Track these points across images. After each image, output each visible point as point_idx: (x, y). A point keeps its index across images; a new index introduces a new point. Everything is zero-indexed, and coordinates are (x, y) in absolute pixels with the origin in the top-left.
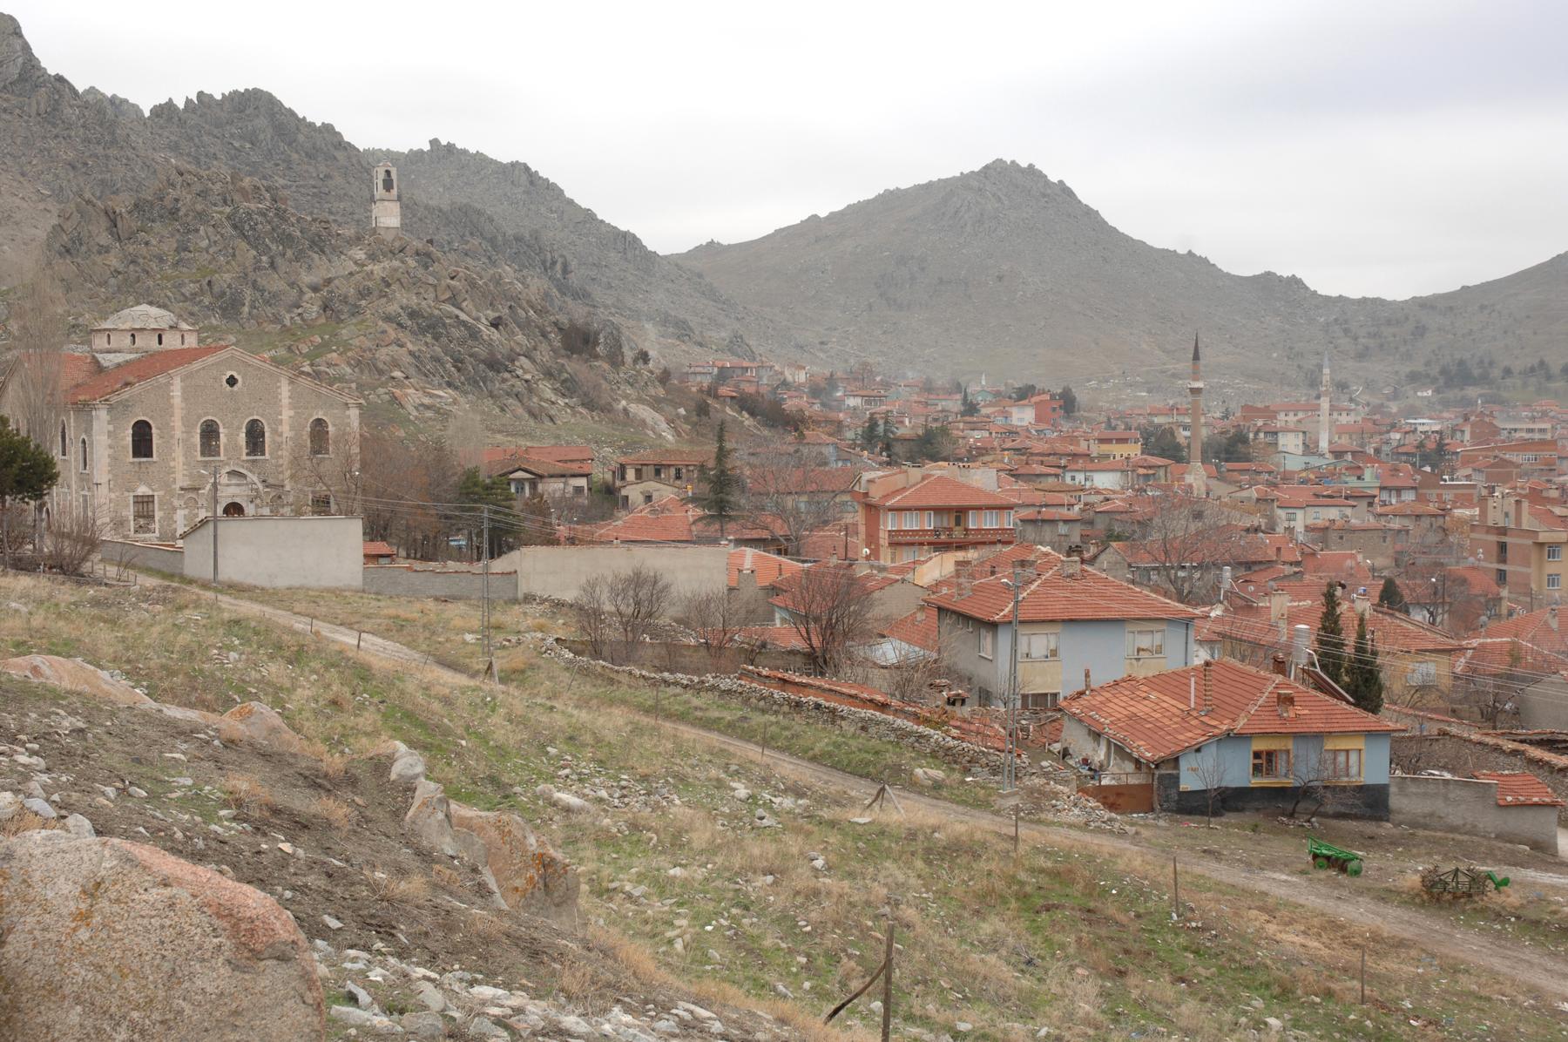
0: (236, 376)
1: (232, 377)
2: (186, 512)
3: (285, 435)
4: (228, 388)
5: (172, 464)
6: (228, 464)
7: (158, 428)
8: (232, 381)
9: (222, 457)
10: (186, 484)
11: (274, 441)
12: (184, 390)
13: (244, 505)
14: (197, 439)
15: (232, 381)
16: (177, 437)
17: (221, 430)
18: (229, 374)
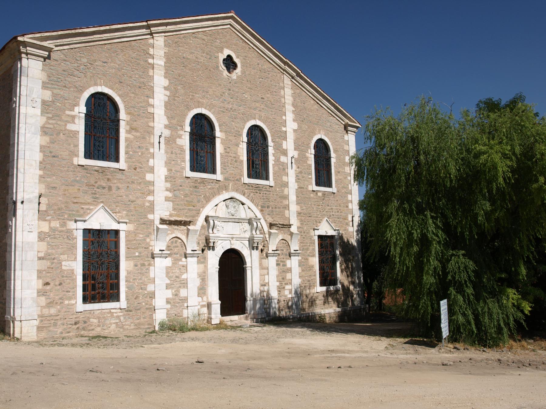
0: (236, 60)
1: (229, 57)
2: (168, 262)
3: (290, 154)
4: (226, 72)
5: (149, 177)
6: (226, 189)
7: (128, 113)
8: (230, 63)
9: (219, 176)
10: (166, 215)
11: (277, 160)
12: (168, 57)
13: (245, 252)
14: (185, 141)
15: (230, 63)
16: (157, 133)
17: (218, 133)
18: (227, 52)
